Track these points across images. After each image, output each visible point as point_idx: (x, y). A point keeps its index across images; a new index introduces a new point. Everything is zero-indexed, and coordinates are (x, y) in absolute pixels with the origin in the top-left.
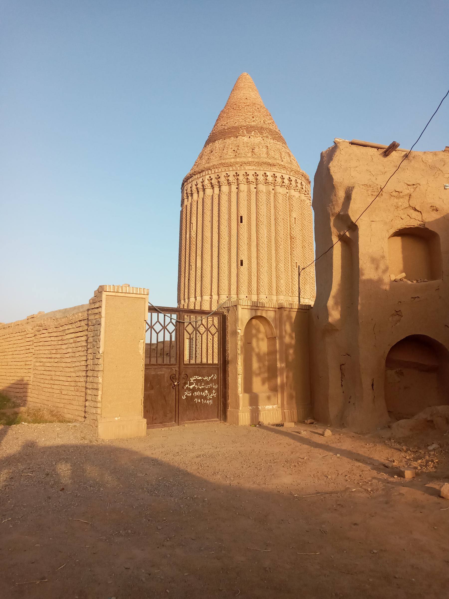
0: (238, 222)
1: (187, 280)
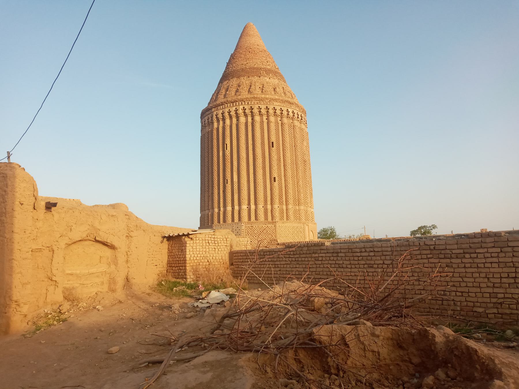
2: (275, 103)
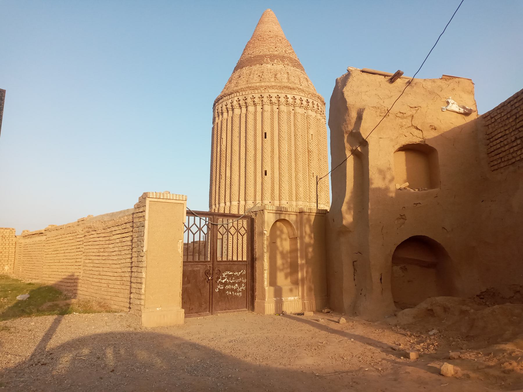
0: (262, 138)
1: (217, 188)
2: (270, 91)
